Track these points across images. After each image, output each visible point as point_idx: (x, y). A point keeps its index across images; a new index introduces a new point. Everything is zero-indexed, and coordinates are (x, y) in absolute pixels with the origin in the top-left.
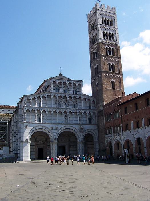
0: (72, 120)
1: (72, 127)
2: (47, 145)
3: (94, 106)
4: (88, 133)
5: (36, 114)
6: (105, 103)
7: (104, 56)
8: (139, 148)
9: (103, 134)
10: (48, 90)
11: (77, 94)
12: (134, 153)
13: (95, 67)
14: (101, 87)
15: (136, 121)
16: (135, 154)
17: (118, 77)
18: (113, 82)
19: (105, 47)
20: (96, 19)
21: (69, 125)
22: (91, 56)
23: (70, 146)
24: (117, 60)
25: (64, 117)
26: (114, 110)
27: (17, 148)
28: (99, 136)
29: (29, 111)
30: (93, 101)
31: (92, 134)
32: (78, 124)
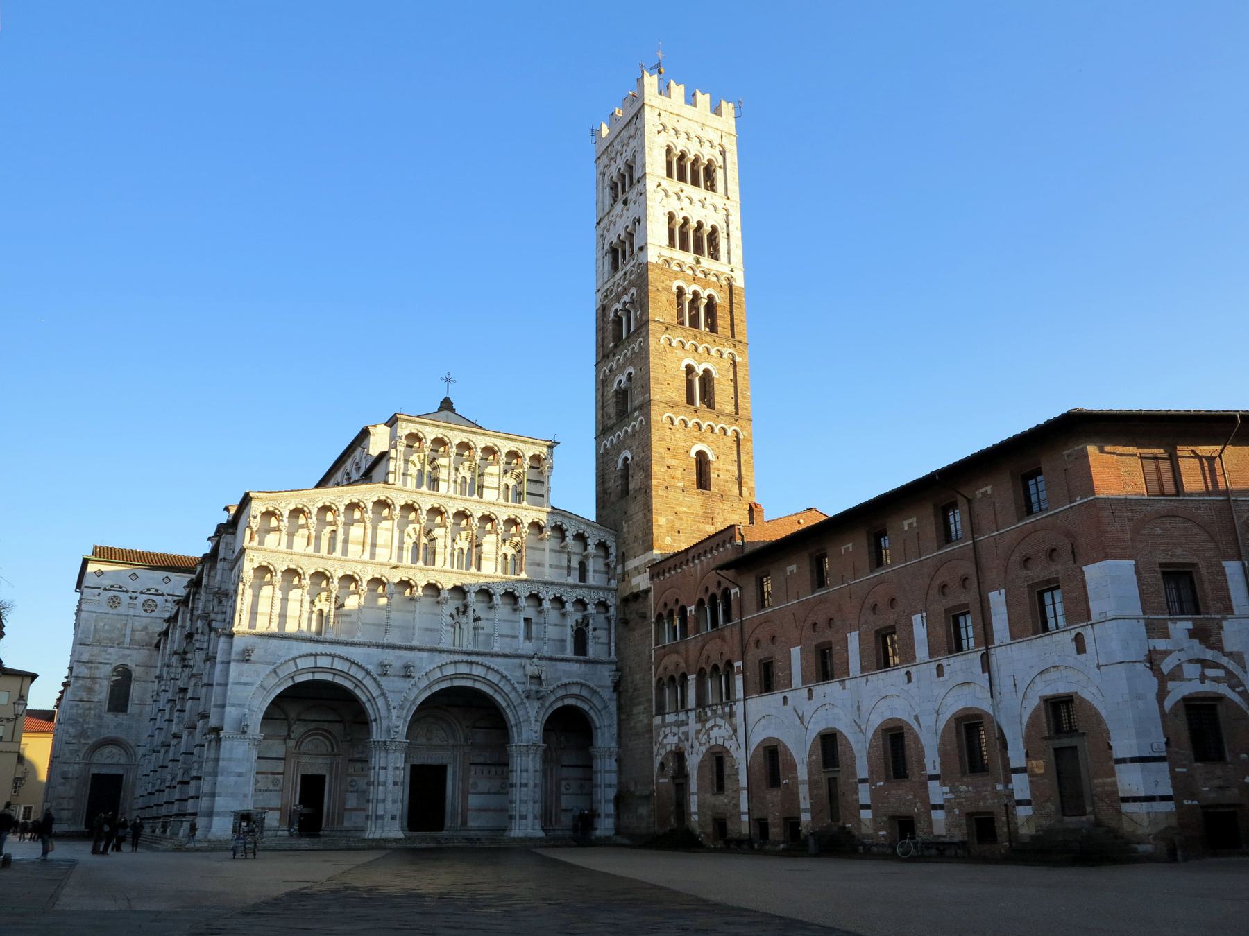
0: (489, 636)
1: (489, 668)
2: (350, 761)
3: (603, 568)
8: (832, 782)
9: (641, 708)
12: (805, 810)
13: (620, 382)
14: (645, 477)
15: (816, 646)
16: (806, 817)
17: (729, 433)
18: (701, 456)
21: (474, 658)
22: (601, 329)
25: (451, 615)
26: (707, 589)
27: (186, 771)
30: (602, 546)
31: (586, 707)
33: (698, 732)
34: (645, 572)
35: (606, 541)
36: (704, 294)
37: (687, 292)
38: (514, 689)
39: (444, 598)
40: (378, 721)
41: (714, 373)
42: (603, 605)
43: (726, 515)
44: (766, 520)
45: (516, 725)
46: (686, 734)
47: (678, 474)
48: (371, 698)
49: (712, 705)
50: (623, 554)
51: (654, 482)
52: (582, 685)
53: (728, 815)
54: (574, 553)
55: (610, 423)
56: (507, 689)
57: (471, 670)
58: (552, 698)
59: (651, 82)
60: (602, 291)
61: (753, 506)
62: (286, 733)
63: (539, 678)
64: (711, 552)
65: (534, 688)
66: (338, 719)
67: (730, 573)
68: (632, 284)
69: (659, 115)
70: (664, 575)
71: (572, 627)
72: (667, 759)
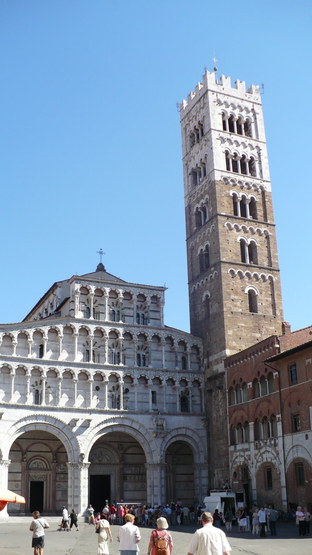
1: (133, 421)
2: (56, 473)
3: (196, 360)
4: (178, 439)
5: (29, 381)
6: (229, 352)
7: (228, 217)
9: (221, 441)
10: (65, 311)
11: (149, 325)
13: (202, 249)
14: (219, 306)
18: (251, 293)
19: (231, 195)
20: (207, 116)
22: (188, 219)
23: (123, 478)
24: (263, 232)
25: (110, 391)
26: (259, 373)
28: (209, 449)
29: (8, 371)
31: (189, 441)
32: (150, 414)
33: (256, 455)
34: (222, 363)
35: (197, 345)
36: (249, 197)
37: (238, 196)
38: (147, 433)
39: (106, 382)
40: (72, 452)
41: (256, 243)
42: (197, 382)
43: (267, 327)
44: (292, 332)
45: (149, 453)
46: (249, 456)
47: (238, 304)
48: (67, 439)
49: (264, 440)
50: (208, 352)
51: (225, 309)
52: (187, 428)
53: (275, 502)
54: (179, 352)
55: (196, 274)
56: (143, 433)
57: (123, 421)
58: (169, 437)
59: (211, 77)
60: (187, 198)
61: (284, 324)
62: (21, 459)
63: (162, 425)
64: (261, 351)
65: (159, 431)
66: (50, 450)
67: (272, 364)
68: (206, 193)
69: (217, 95)
70: (232, 365)
71: (179, 395)
72: (238, 470)
